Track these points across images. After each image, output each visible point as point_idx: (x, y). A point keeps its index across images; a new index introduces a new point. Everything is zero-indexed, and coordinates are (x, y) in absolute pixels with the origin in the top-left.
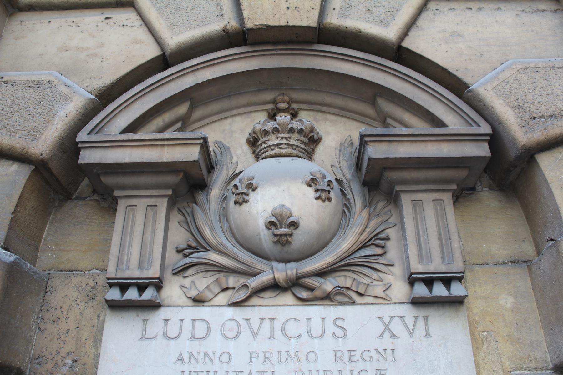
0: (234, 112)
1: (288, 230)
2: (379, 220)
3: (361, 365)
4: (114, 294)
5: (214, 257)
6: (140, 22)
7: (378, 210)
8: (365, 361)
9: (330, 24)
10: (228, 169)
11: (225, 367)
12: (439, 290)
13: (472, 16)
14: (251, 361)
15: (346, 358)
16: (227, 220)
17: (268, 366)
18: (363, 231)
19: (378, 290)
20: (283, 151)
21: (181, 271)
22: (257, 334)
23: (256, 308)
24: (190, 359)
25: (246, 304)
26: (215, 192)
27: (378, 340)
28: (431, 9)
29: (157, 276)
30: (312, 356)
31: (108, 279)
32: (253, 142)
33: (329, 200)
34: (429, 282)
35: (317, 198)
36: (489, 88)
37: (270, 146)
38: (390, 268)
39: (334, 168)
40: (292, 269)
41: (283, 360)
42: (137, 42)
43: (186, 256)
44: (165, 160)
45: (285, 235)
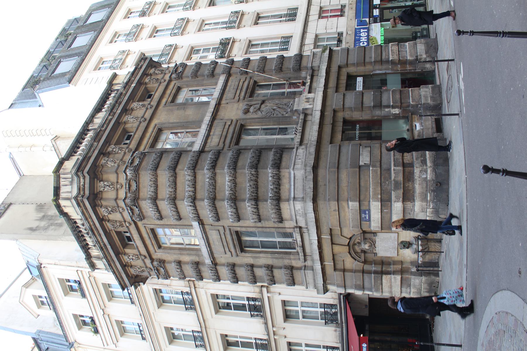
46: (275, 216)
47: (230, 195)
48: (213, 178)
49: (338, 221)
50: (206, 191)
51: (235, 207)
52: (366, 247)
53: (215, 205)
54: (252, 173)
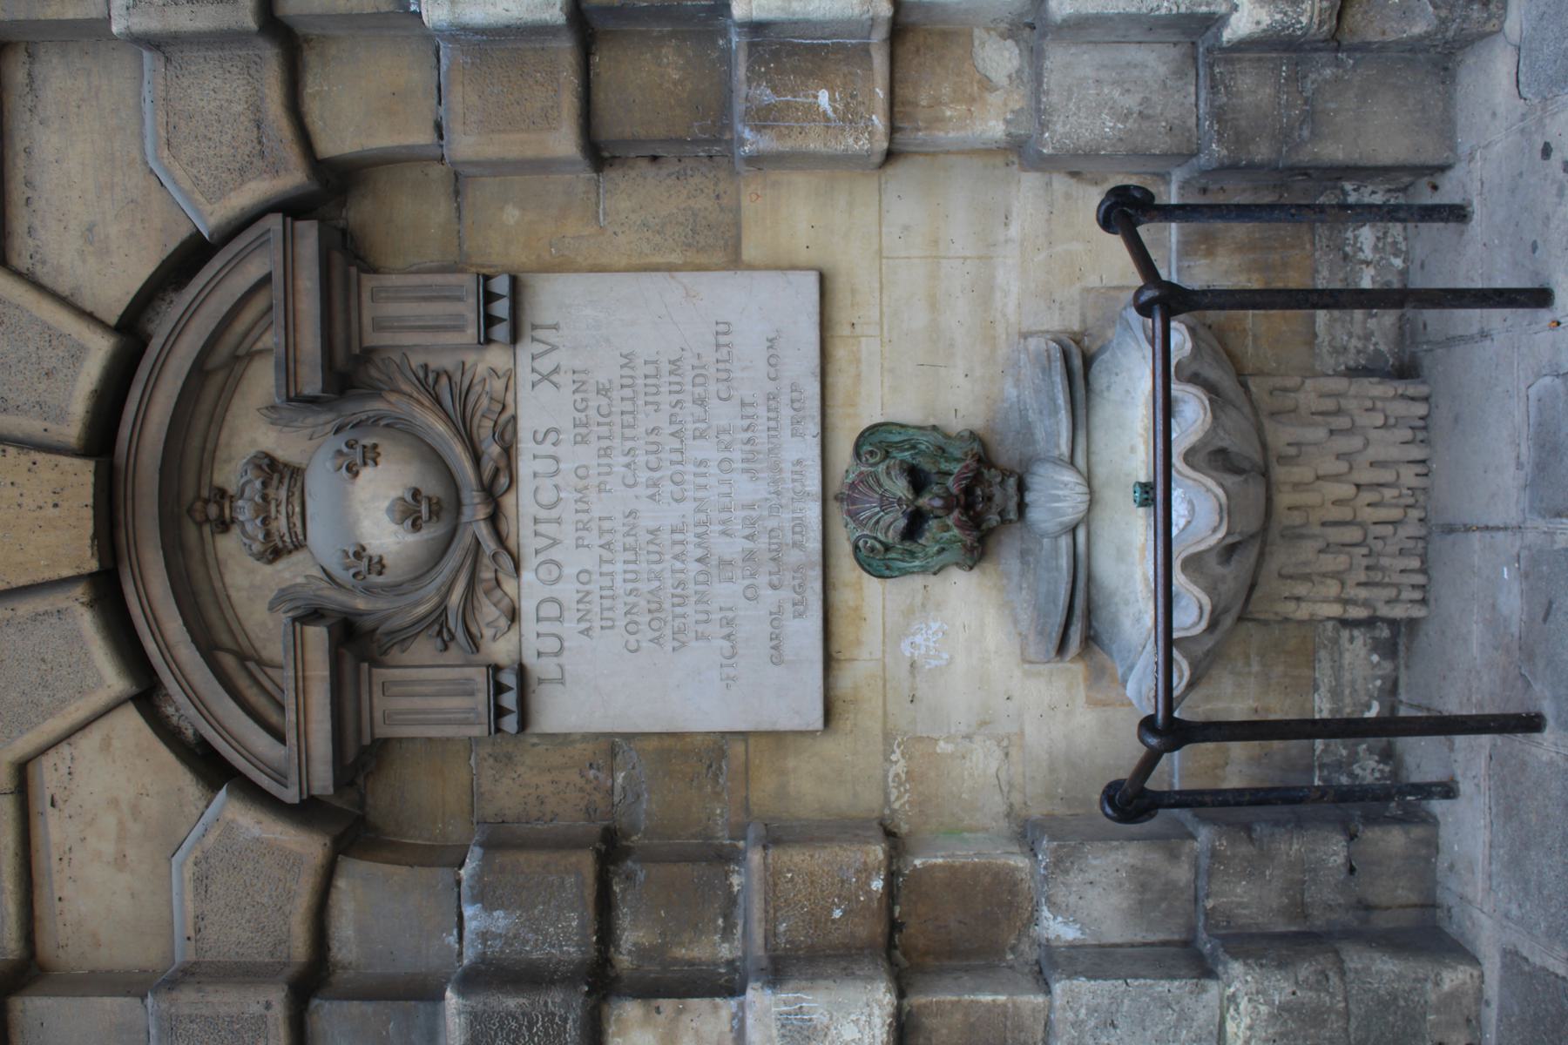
0: (218, 585)
1: (423, 502)
2: (398, 376)
3: (592, 412)
4: (510, 723)
5: (456, 598)
6: (65, 749)
7: (384, 378)
8: (587, 407)
9: (79, 438)
10: (322, 589)
11: (595, 577)
12: (501, 308)
13: (47, 200)
14: (588, 546)
15: (583, 431)
16: (400, 585)
17: (594, 525)
18: (418, 401)
19: (498, 385)
20: (297, 509)
21: (474, 642)
22: (554, 539)
23: (522, 541)
24: (586, 620)
25: (516, 555)
26: (361, 604)
27: (561, 390)
28: (30, 266)
29: (484, 669)
30: (581, 472)
31: (490, 733)
32: (275, 553)
33: (375, 446)
34: (490, 321)
35: (376, 464)
36: (209, 208)
37: (289, 529)
38: (467, 366)
39: (315, 436)
40: (473, 497)
41: (585, 507)
42: (106, 745)
43: (453, 637)
44: (327, 673)
45: (430, 506)
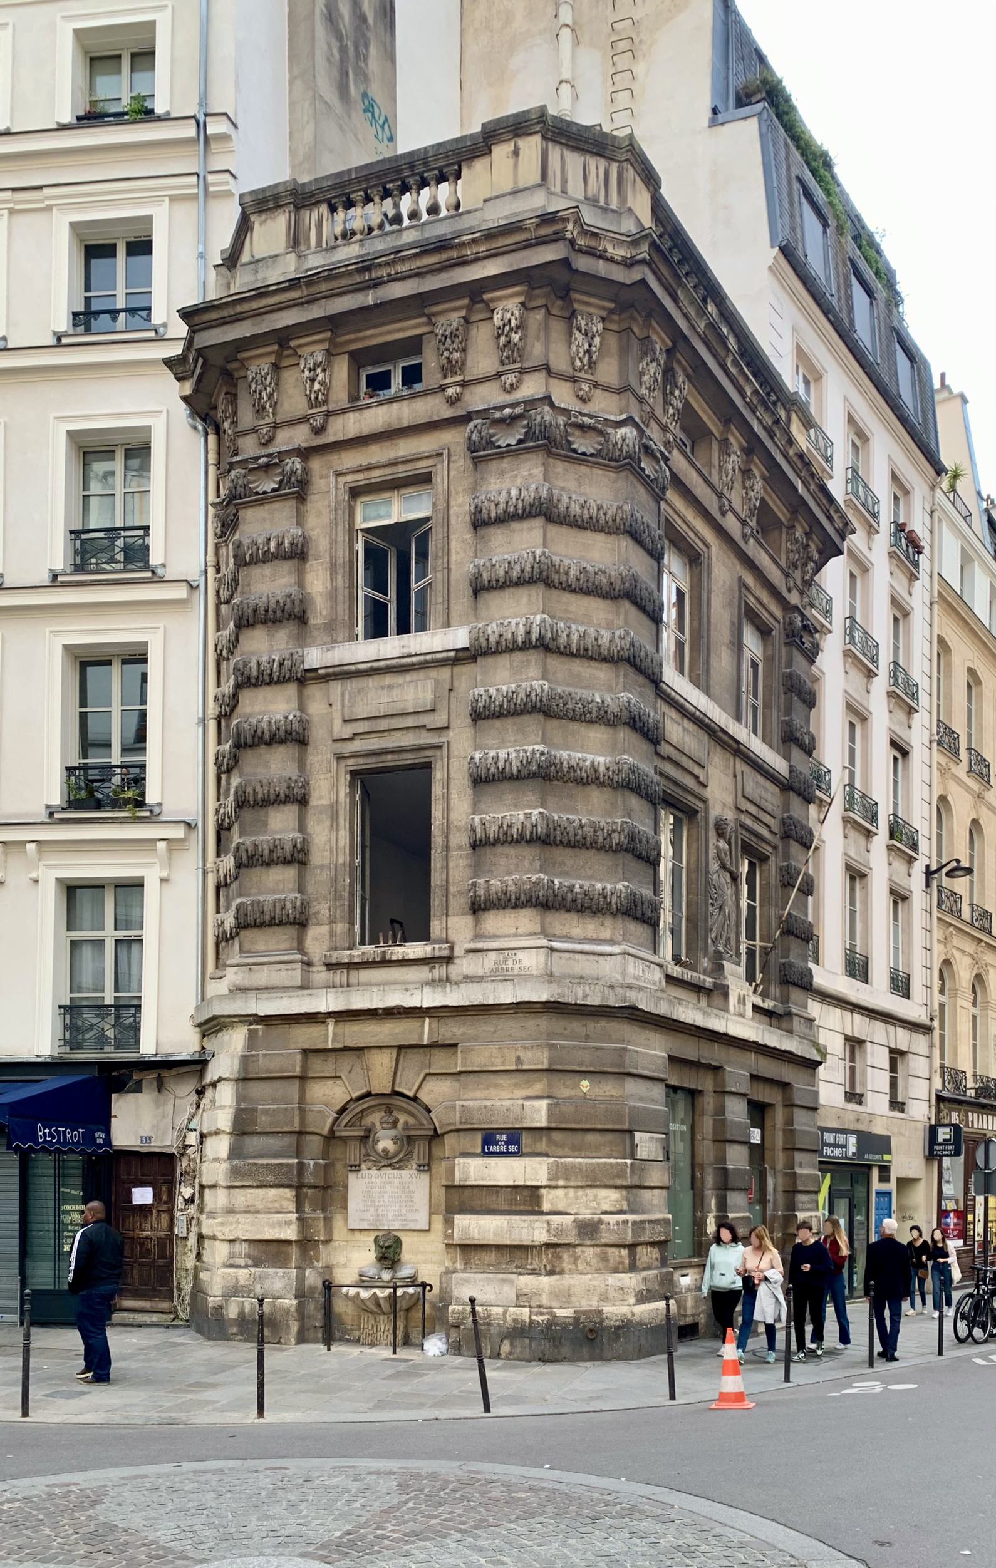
32: (381, 1123)
46: (493, 889)
47: (557, 761)
48: (603, 718)
49: (485, 1069)
50: (568, 689)
51: (524, 772)
52: (385, 1143)
53: (530, 713)
54: (615, 835)
